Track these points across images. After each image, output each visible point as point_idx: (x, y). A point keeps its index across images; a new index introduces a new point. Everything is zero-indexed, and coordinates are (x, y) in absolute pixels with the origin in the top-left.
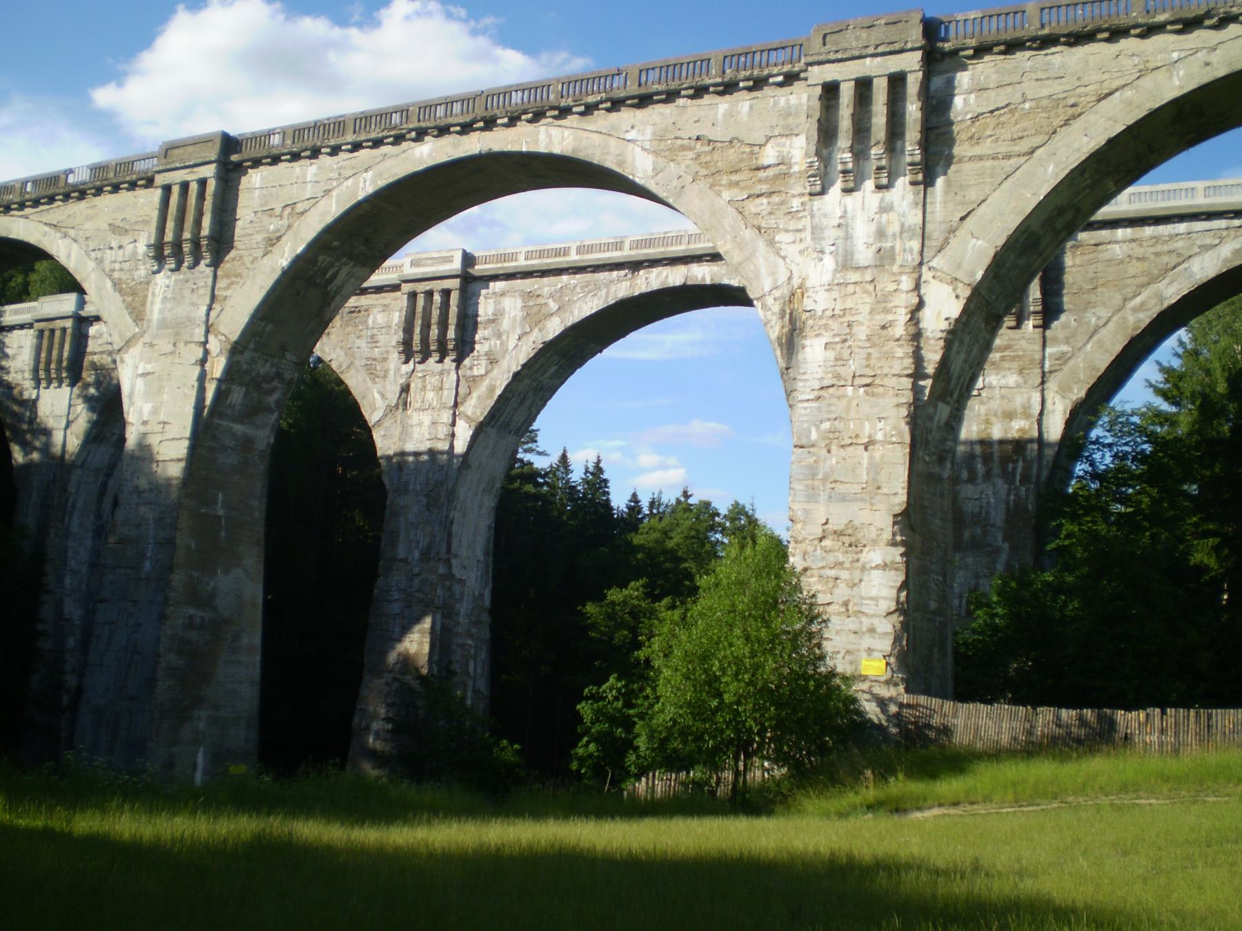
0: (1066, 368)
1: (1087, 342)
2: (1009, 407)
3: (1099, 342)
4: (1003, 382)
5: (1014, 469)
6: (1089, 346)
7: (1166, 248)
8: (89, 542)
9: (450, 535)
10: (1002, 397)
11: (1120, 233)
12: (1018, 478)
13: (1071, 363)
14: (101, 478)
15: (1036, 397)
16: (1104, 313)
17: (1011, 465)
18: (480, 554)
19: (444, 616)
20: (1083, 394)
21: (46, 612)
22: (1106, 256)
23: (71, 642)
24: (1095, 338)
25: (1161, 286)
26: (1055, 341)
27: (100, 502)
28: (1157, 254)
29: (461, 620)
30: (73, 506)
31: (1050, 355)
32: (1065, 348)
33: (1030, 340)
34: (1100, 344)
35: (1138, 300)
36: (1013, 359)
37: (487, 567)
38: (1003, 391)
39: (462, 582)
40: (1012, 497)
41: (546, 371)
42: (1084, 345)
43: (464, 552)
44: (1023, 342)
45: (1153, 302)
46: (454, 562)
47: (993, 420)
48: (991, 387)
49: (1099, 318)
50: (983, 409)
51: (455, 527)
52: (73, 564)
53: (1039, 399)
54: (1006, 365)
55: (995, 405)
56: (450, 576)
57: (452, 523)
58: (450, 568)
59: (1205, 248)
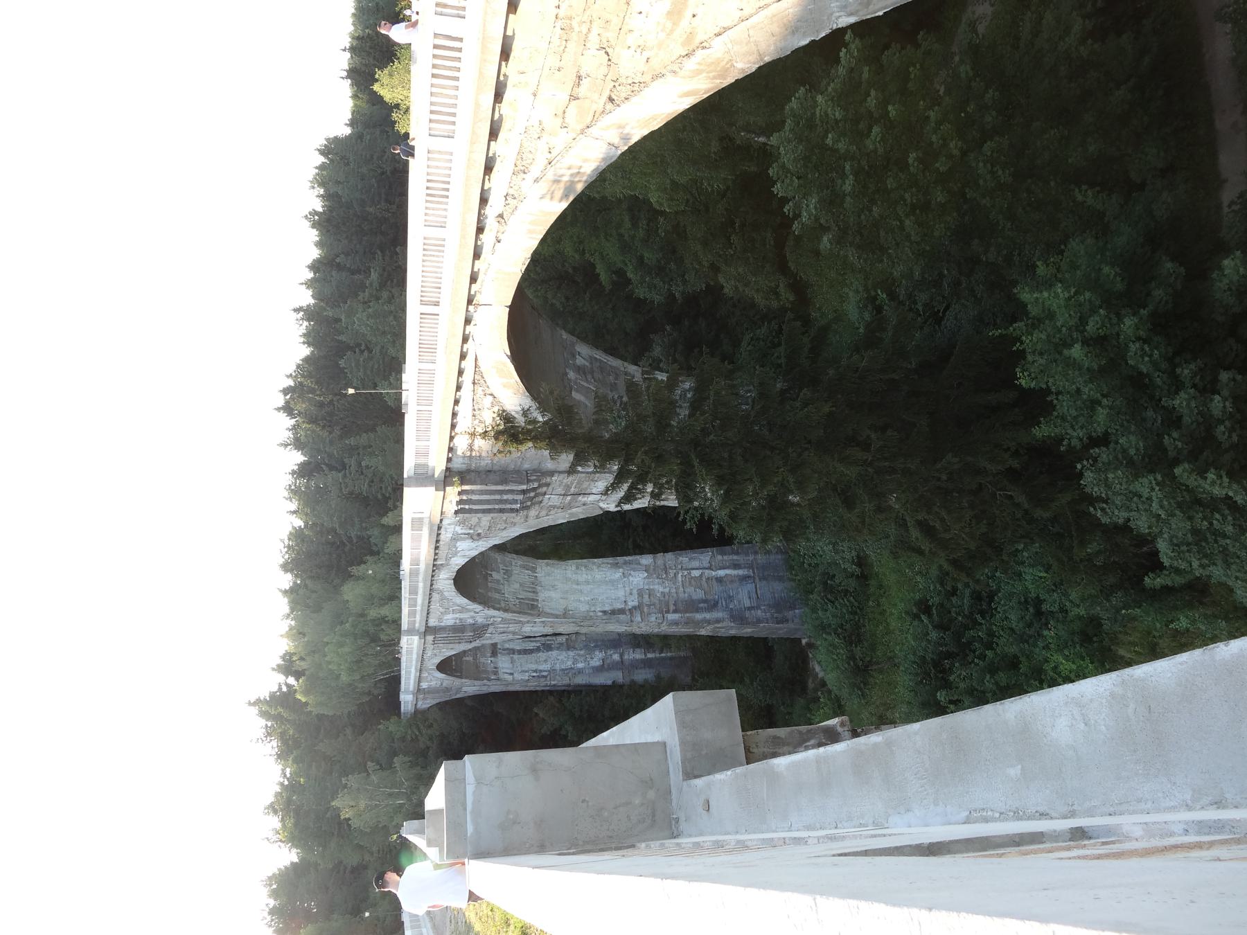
8: (555, 653)
9: (613, 612)
14: (516, 656)
18: (618, 574)
19: (668, 612)
21: (604, 679)
23: (616, 657)
27: (531, 652)
29: (667, 590)
30: (535, 671)
37: (625, 563)
39: (640, 593)
41: (498, 581)
43: (621, 593)
46: (631, 604)
51: (607, 608)
52: (569, 663)
56: (639, 607)
57: (604, 612)
58: (635, 608)
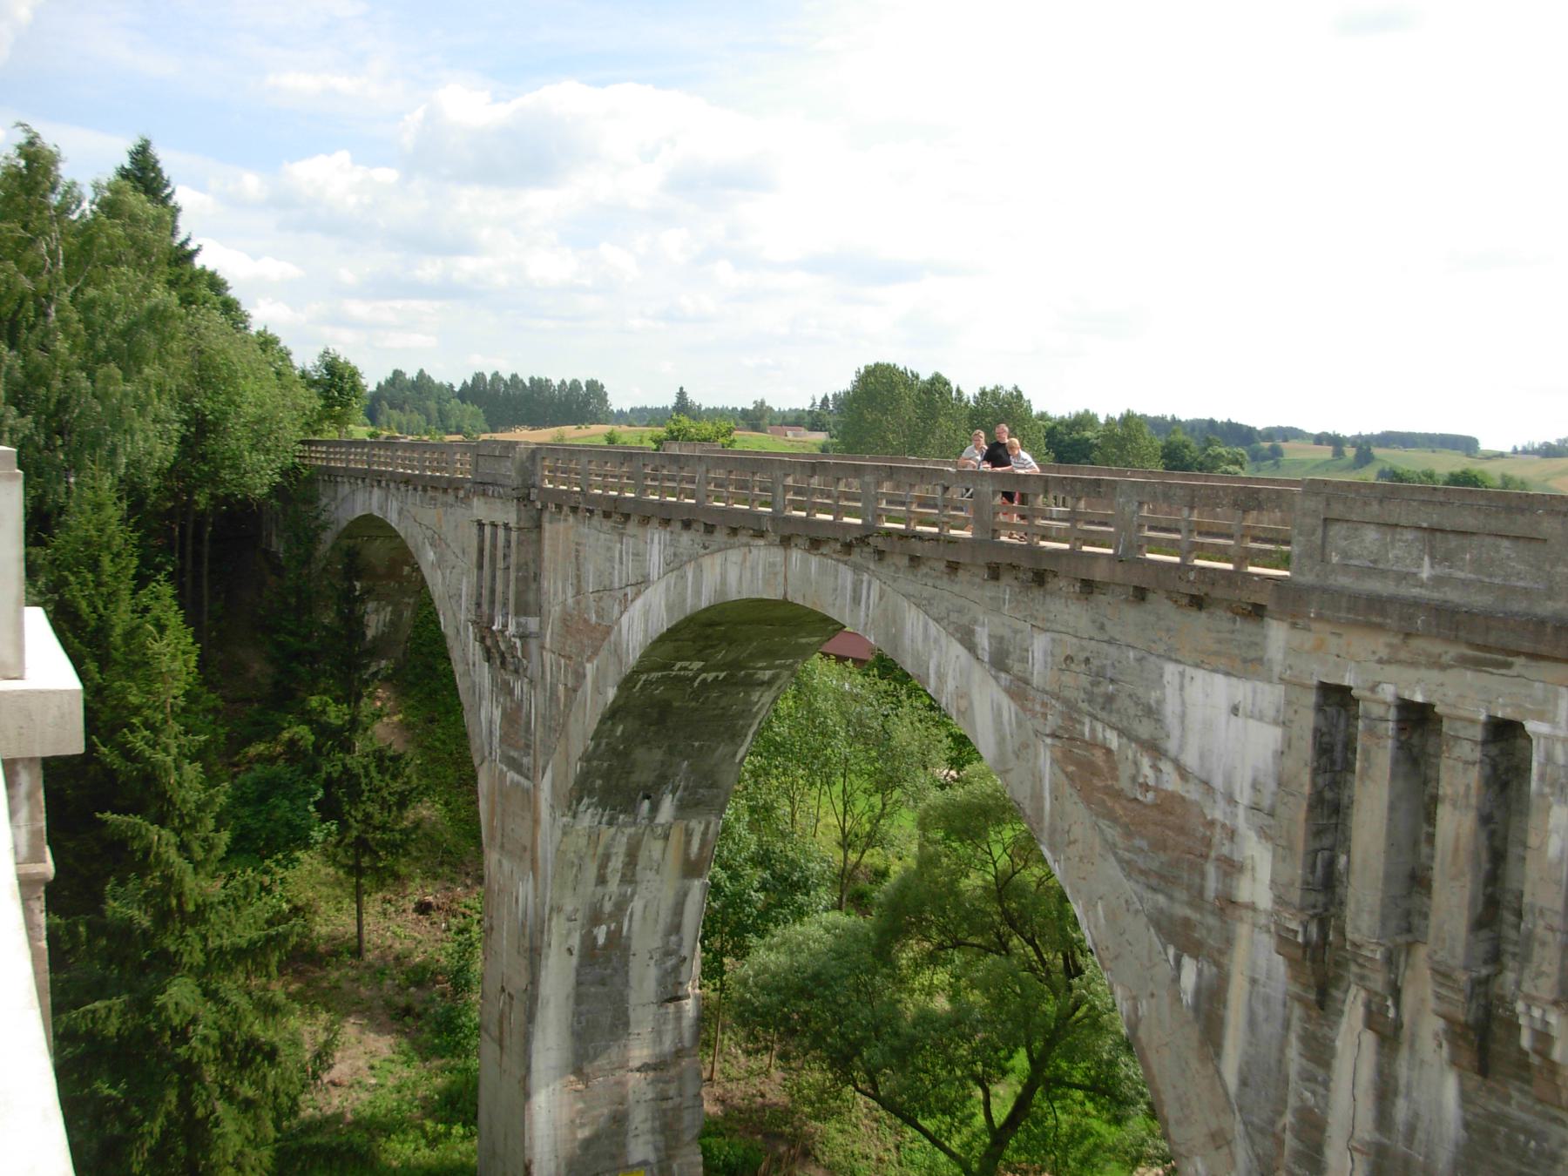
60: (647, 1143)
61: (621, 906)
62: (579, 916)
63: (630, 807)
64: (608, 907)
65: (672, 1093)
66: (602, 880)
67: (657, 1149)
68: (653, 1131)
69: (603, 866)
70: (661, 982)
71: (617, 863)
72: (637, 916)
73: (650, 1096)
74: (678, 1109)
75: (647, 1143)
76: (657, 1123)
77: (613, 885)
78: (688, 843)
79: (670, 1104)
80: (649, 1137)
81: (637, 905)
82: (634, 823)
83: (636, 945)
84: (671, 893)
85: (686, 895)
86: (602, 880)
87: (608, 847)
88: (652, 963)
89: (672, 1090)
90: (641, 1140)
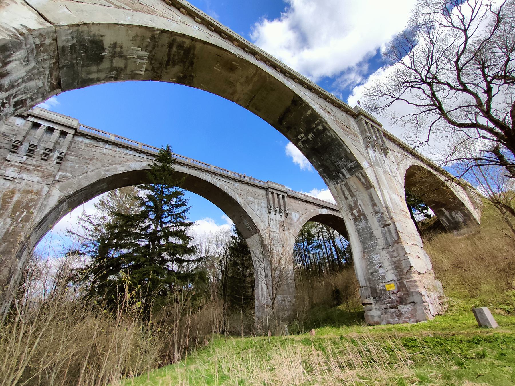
0: (66, 182)
1: (81, 175)
2: (30, 189)
3: (86, 176)
4: (30, 179)
5: (19, 216)
6: (80, 177)
7: (123, 156)
10: (27, 184)
11: (107, 146)
12: (20, 219)
13: (71, 180)
15: (46, 189)
16: (91, 167)
17: (18, 213)
20: (71, 193)
22: (99, 151)
24: (85, 175)
25: (118, 166)
26: (66, 171)
28: (120, 157)
31: (60, 175)
32: (69, 175)
33: (53, 167)
34: (86, 177)
35: (107, 168)
36: (40, 171)
38: (28, 182)
40: (12, 227)
42: (79, 176)
44: (49, 167)
45: (113, 170)
47: (17, 192)
48: (21, 178)
49: (89, 169)
50: (12, 187)
53: (48, 189)
54: (35, 172)
55: (20, 186)
59: (137, 161)
60: (392, 273)
61: (356, 203)
62: (347, 209)
63: (338, 177)
64: (353, 205)
65: (395, 255)
66: (346, 198)
67: (396, 275)
68: (393, 269)
69: (344, 195)
70: (379, 221)
71: (347, 193)
72: (362, 205)
73: (388, 257)
74: (399, 260)
75: (392, 273)
76: (393, 266)
77: (349, 197)
78: (360, 179)
79: (396, 259)
80: (392, 271)
81: (359, 202)
82: (343, 181)
83: (366, 213)
84: (367, 195)
85: (371, 194)
86: (346, 198)
87: (341, 189)
88: (373, 216)
89: (395, 254)
90: (390, 272)
